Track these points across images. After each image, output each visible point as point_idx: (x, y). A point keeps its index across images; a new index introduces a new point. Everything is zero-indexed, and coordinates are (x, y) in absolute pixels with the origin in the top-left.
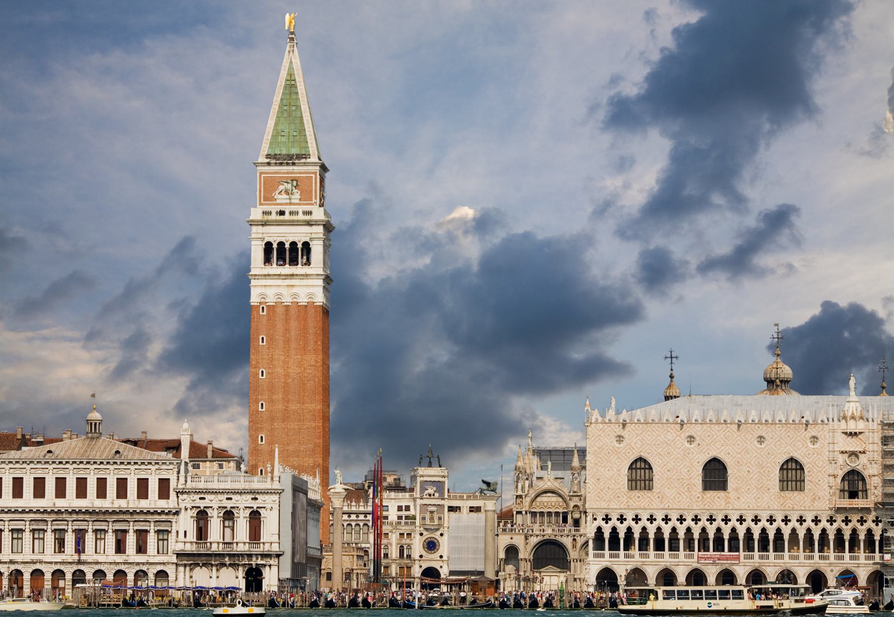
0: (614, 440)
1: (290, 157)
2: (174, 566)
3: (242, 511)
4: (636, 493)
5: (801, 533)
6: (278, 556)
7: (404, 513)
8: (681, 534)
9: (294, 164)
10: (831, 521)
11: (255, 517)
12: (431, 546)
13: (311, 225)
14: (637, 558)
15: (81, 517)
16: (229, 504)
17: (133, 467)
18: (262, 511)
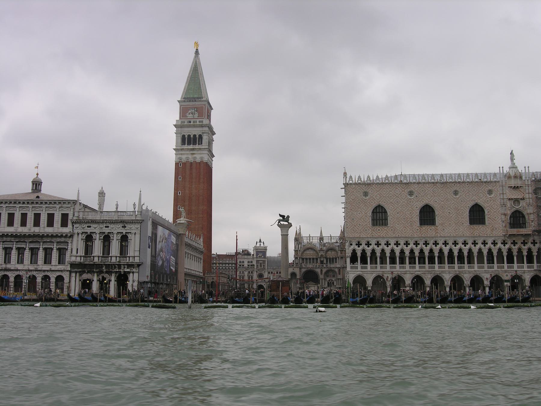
0: (362, 194)
1: (194, 98)
2: (68, 273)
3: (115, 235)
4: (378, 228)
5: (485, 252)
6: (139, 266)
7: (250, 264)
8: (407, 253)
9: (195, 101)
10: (504, 243)
11: (124, 239)
12: (261, 276)
13: (203, 127)
14: (379, 269)
15: (9, 239)
16: (107, 231)
17: (44, 206)
18: (129, 236)
